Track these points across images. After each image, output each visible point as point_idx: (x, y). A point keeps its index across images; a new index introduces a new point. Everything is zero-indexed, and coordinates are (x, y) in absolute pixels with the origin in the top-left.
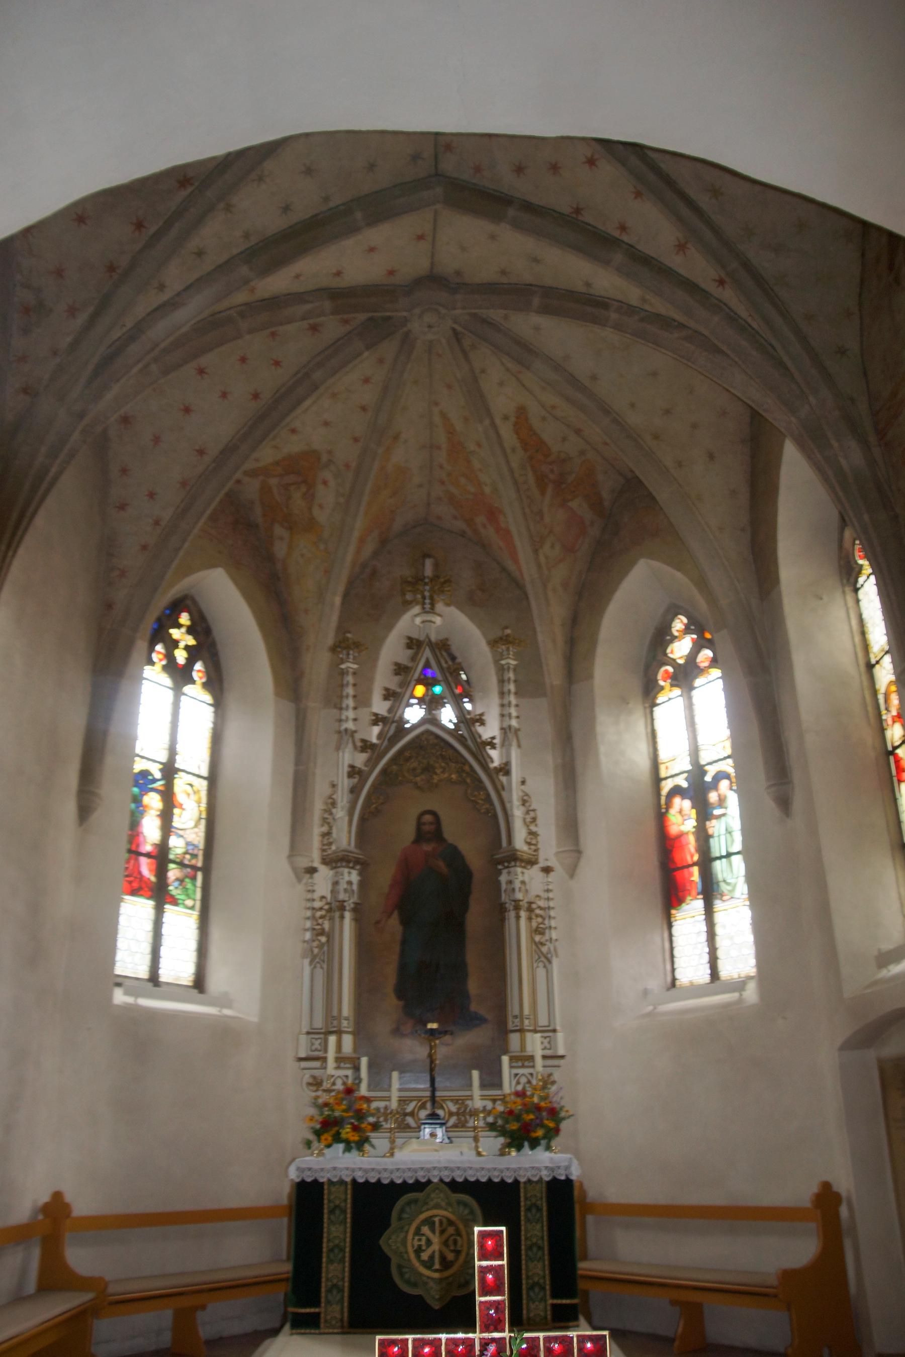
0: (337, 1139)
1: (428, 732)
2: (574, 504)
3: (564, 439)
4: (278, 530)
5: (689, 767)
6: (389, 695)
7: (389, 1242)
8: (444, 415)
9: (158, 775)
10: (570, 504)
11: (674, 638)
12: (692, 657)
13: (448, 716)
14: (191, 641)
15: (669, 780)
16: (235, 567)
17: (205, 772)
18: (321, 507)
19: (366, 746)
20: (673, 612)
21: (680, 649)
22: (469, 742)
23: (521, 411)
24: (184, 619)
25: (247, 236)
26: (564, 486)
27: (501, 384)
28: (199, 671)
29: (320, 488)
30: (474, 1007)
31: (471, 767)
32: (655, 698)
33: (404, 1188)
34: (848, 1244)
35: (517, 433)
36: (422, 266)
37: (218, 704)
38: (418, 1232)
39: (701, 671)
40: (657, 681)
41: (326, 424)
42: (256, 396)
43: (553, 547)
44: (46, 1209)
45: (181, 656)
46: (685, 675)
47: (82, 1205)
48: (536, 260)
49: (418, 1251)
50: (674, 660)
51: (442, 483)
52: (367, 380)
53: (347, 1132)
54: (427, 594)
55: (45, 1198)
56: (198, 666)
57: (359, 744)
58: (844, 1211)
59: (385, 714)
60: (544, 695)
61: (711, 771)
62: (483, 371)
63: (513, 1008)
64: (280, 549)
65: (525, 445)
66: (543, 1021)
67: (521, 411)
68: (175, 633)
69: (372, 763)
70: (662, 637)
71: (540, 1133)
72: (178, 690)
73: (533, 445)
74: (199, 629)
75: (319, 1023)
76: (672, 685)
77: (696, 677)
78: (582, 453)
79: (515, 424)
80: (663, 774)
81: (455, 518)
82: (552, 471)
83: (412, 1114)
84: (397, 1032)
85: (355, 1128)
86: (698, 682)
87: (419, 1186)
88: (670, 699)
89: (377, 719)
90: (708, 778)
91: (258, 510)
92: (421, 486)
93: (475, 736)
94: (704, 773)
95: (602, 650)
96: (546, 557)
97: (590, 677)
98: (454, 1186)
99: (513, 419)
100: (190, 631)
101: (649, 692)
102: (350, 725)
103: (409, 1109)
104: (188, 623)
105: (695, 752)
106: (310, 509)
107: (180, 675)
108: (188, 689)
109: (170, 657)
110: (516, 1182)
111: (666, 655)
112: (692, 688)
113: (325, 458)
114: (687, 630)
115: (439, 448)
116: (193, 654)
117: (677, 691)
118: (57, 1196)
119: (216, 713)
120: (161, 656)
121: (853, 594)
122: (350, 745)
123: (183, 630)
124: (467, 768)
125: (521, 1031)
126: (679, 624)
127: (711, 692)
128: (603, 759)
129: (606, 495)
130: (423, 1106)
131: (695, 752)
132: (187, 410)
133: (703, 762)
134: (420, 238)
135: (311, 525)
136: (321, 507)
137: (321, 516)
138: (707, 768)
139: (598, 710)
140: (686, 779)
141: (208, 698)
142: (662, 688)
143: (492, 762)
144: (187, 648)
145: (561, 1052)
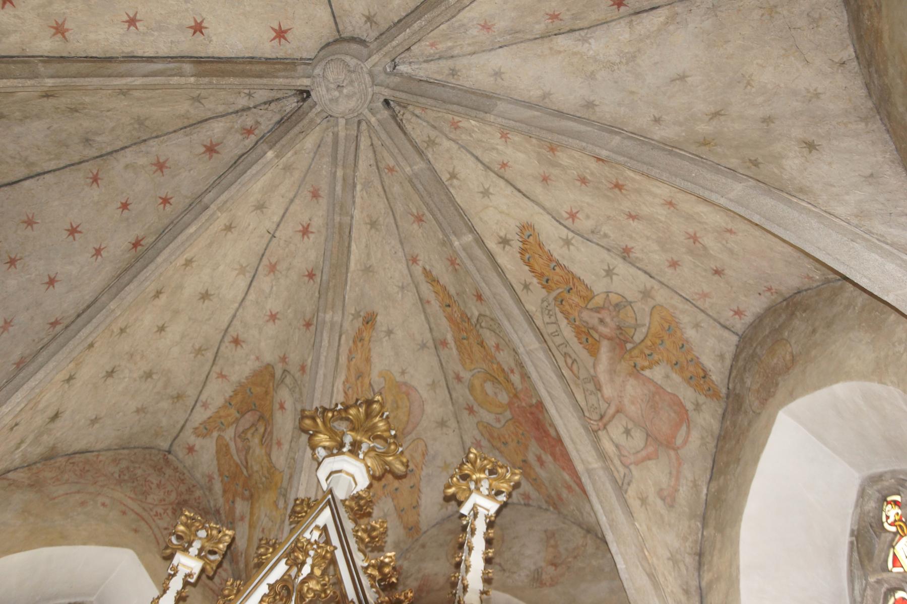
2: (657, 374)
3: (609, 273)
8: (427, 273)
10: (647, 373)
23: (527, 231)
26: (629, 346)
29: (278, 415)
35: (528, 263)
36: (327, 32)
41: (273, 317)
43: (627, 432)
62: (453, 176)
65: (547, 283)
67: (527, 231)
78: (646, 294)
79: (523, 251)
82: (601, 321)
96: (617, 446)
99: (517, 244)
111: (885, 569)
113: (278, 373)
115: (444, 343)
129: (708, 361)
132: (52, 282)
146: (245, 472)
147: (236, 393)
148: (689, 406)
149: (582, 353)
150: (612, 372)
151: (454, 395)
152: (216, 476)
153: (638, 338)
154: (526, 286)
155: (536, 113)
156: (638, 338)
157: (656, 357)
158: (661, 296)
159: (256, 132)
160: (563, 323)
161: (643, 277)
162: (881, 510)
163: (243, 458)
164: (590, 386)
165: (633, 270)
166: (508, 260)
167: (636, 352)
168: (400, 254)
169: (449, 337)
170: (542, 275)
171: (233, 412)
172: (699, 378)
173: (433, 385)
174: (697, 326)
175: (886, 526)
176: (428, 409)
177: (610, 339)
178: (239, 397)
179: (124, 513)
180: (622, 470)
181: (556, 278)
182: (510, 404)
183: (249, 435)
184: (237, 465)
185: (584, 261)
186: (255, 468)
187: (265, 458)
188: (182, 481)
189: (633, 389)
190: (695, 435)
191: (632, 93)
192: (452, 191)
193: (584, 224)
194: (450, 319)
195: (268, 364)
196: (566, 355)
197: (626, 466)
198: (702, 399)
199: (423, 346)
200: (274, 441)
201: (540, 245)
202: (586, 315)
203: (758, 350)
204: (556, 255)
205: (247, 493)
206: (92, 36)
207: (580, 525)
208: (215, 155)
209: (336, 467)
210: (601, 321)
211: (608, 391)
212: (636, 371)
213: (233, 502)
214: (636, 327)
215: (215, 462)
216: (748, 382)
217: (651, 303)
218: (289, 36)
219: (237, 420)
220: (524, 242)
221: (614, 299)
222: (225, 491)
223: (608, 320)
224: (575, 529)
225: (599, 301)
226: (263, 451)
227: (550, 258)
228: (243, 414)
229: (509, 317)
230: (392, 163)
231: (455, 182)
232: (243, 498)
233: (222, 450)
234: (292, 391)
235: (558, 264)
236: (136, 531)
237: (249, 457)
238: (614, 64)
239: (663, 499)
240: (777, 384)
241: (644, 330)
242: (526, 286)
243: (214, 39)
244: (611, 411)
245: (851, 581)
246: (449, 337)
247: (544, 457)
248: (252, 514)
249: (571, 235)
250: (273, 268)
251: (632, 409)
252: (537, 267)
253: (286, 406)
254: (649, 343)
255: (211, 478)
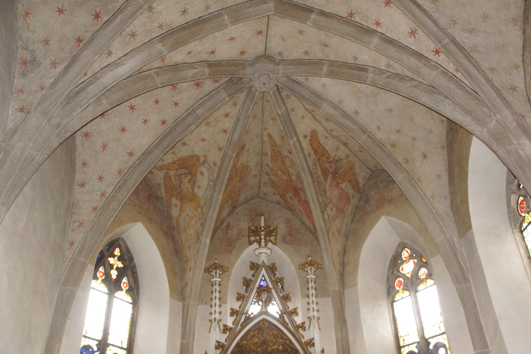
1: (264, 320)
2: (343, 186)
3: (337, 149)
4: (174, 201)
5: (418, 340)
6: (240, 297)
8: (269, 135)
9: (95, 349)
10: (341, 185)
11: (403, 262)
12: (415, 274)
13: (274, 309)
14: (120, 265)
15: (406, 347)
16: (149, 221)
17: (125, 346)
18: (199, 187)
19: (226, 329)
20: (402, 246)
21: (408, 268)
22: (290, 326)
23: (314, 133)
24: (117, 252)
25: (161, 26)
26: (337, 175)
27: (303, 117)
28: (124, 283)
29: (199, 177)
31: (290, 341)
32: (394, 297)
35: (311, 145)
36: (261, 50)
37: (135, 303)
39: (422, 281)
40: (395, 287)
41: (203, 140)
42: (164, 123)
43: (332, 209)
45: (114, 274)
46: (412, 284)
48: (326, 45)
50: (405, 275)
51: (268, 174)
52: (227, 115)
54: (263, 237)
56: (125, 280)
57: (222, 328)
59: (238, 308)
60: (328, 296)
61: (433, 342)
64: (175, 212)
65: (316, 152)
67: (314, 133)
68: (111, 260)
69: (230, 339)
70: (396, 261)
72: (111, 294)
73: (319, 151)
74: (126, 257)
76: (403, 290)
77: (419, 284)
79: (311, 140)
80: (402, 344)
81: (275, 194)
82: (331, 166)
86: (421, 287)
88: (402, 298)
89: (233, 313)
90: (431, 347)
91: (163, 189)
92: (255, 176)
93: (293, 322)
94: (428, 344)
95: (361, 269)
96: (328, 216)
97: (356, 285)
99: (309, 138)
100: (120, 259)
101: (391, 293)
102: (217, 316)
104: (119, 254)
105: (421, 331)
106: (193, 189)
107: (113, 286)
108: (118, 294)
109: (107, 275)
111: (399, 271)
112: (416, 291)
113: (202, 159)
114: (411, 257)
115: (266, 154)
116: (121, 272)
117: (407, 293)
119: (134, 308)
120: (101, 274)
121: (520, 234)
122: (218, 329)
123: (116, 258)
124: (287, 342)
126: (405, 254)
127: (430, 294)
128: (365, 335)
129: (360, 180)
131: (421, 331)
132: (123, 130)
133: (427, 337)
134: (260, 33)
135: (194, 198)
136: (199, 187)
137: (200, 193)
138: (430, 340)
139: (360, 305)
140: (417, 347)
141: (130, 300)
142: (398, 291)
143: (303, 337)
144: (118, 269)
146: (179, 189)
147: (178, 160)
148: (351, 196)
149: (322, 178)
150: (331, 186)
151: (263, 169)
152: (162, 184)
153: (340, 172)
154: (309, 155)
155: (337, 113)
156: (340, 172)
157: (345, 179)
158: (352, 158)
159: (219, 82)
160: (319, 168)
161: (348, 151)
162: (402, 251)
163: (178, 184)
164: (323, 193)
165: (346, 149)
166: (305, 144)
167: (339, 178)
168: (260, 126)
169: (269, 153)
170: (315, 149)
171: (176, 166)
172: (356, 186)
173: (256, 166)
174: (360, 168)
175: (403, 257)
176: (252, 172)
177: (332, 173)
178: (180, 162)
179: (135, 206)
180: (329, 224)
181: (319, 150)
182: (286, 180)
183: (183, 177)
184: (174, 185)
185: (330, 145)
186: (184, 190)
187: (190, 189)
188: (148, 185)
189: (336, 192)
190: (350, 206)
191: (372, 111)
192: (291, 116)
193: (335, 133)
194: (272, 149)
195: (196, 156)
196: (318, 181)
197: (330, 223)
198: (355, 193)
199: (258, 154)
200: (196, 184)
201: (317, 138)
202: (326, 164)
203: (379, 183)
204: (321, 142)
205: (179, 197)
206: (173, 59)
207: (300, 220)
208: (199, 87)
209: (260, 252)
210: (331, 166)
211: (328, 194)
212: (337, 186)
213: (171, 197)
214: (340, 168)
215: (163, 180)
216: (373, 194)
217: (348, 159)
218: (245, 54)
219: (177, 170)
220: (311, 137)
221: (337, 158)
222: (166, 192)
223: (333, 166)
224: (297, 220)
225: (331, 159)
226: (190, 186)
227: (319, 143)
228: (180, 168)
229: (304, 171)
230: (269, 99)
231: (293, 112)
232: (177, 198)
233: (167, 177)
234: (208, 170)
235: (321, 145)
236: (140, 213)
237: (181, 185)
238: (368, 96)
239: (338, 232)
240: (384, 205)
241: (343, 169)
242: (309, 155)
243: (217, 55)
244: (328, 202)
245: (388, 270)
246: (269, 153)
247: (294, 198)
248: (181, 206)
249: (328, 135)
250: (208, 124)
251: (334, 200)
252: (314, 147)
253: (204, 174)
254: (343, 174)
255: (159, 185)
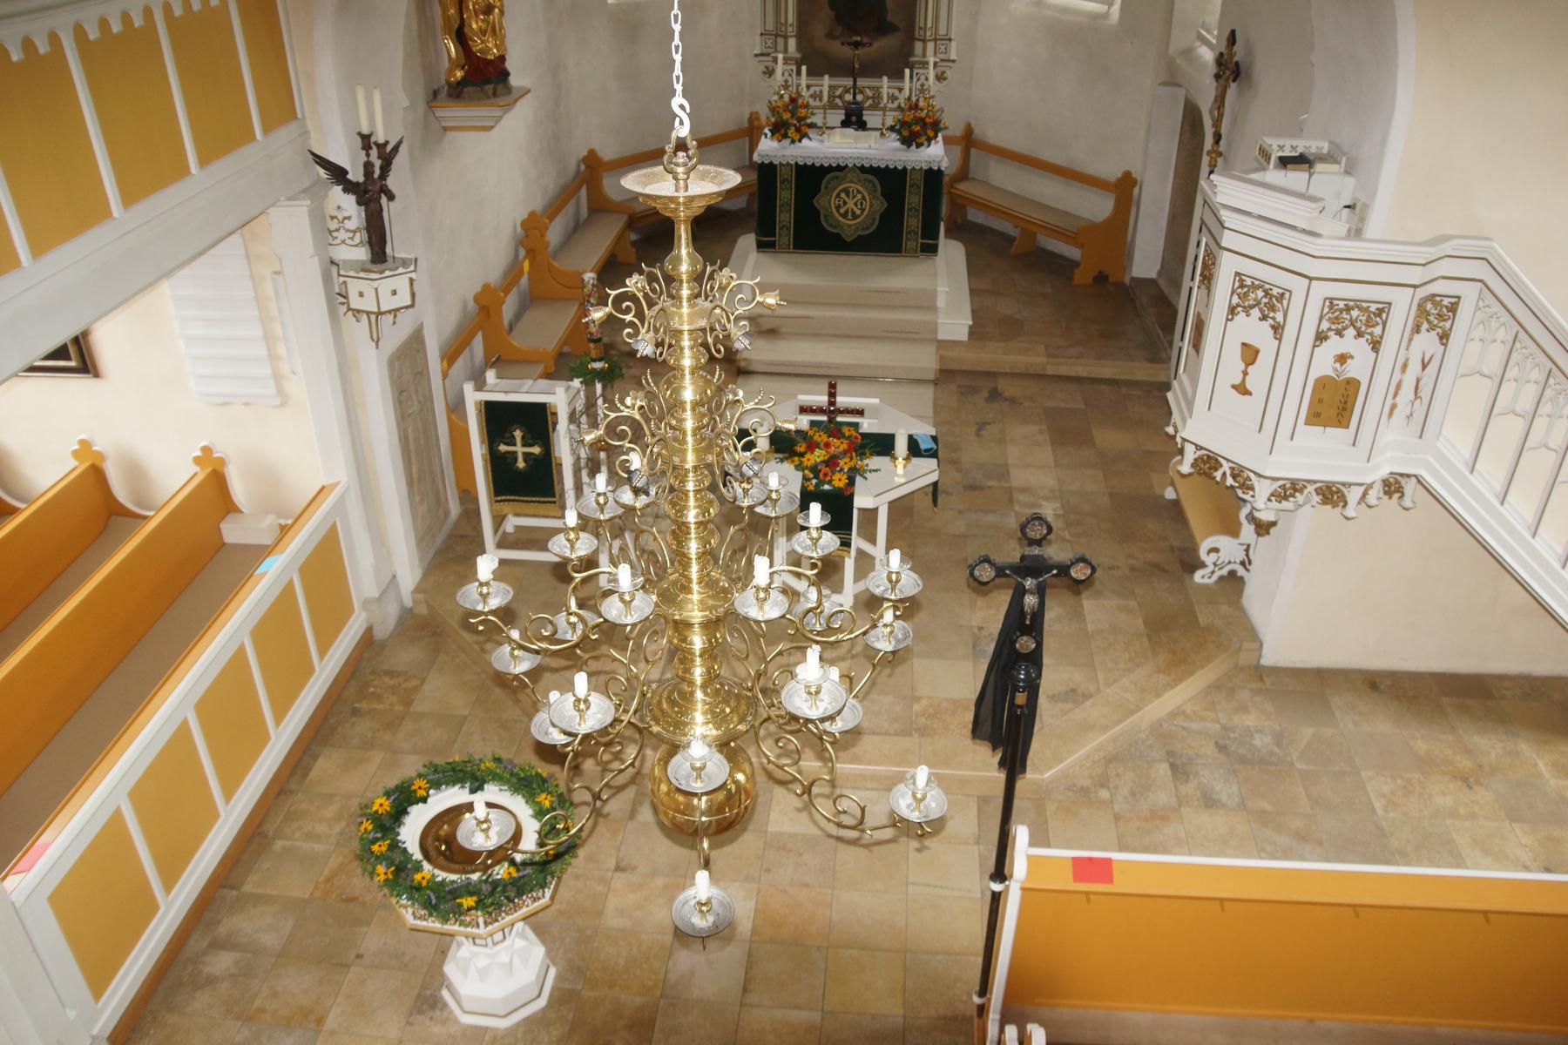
0: (785, 136)
7: (820, 202)
30: (890, 18)
33: (830, 169)
34: (1134, 209)
38: (838, 196)
44: (585, 160)
47: (607, 153)
49: (838, 208)
53: (791, 131)
55: (585, 153)
58: (1136, 191)
63: (920, 22)
66: (942, 31)
71: (923, 139)
75: (770, 26)
83: (840, 97)
84: (830, 35)
85: (798, 130)
87: (839, 168)
98: (863, 169)
103: (838, 93)
110: (905, 169)
118: (592, 153)
125: (924, 41)
130: (847, 91)
145: (953, 57)
